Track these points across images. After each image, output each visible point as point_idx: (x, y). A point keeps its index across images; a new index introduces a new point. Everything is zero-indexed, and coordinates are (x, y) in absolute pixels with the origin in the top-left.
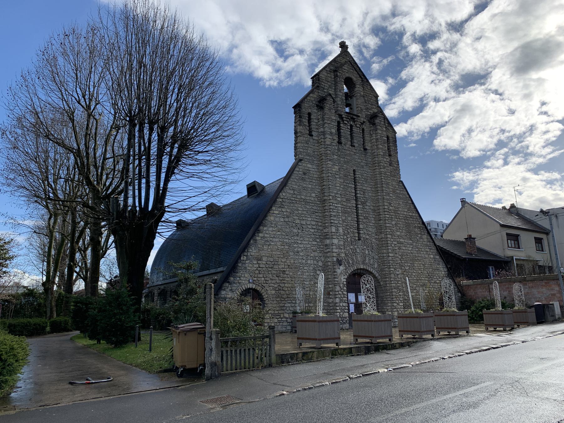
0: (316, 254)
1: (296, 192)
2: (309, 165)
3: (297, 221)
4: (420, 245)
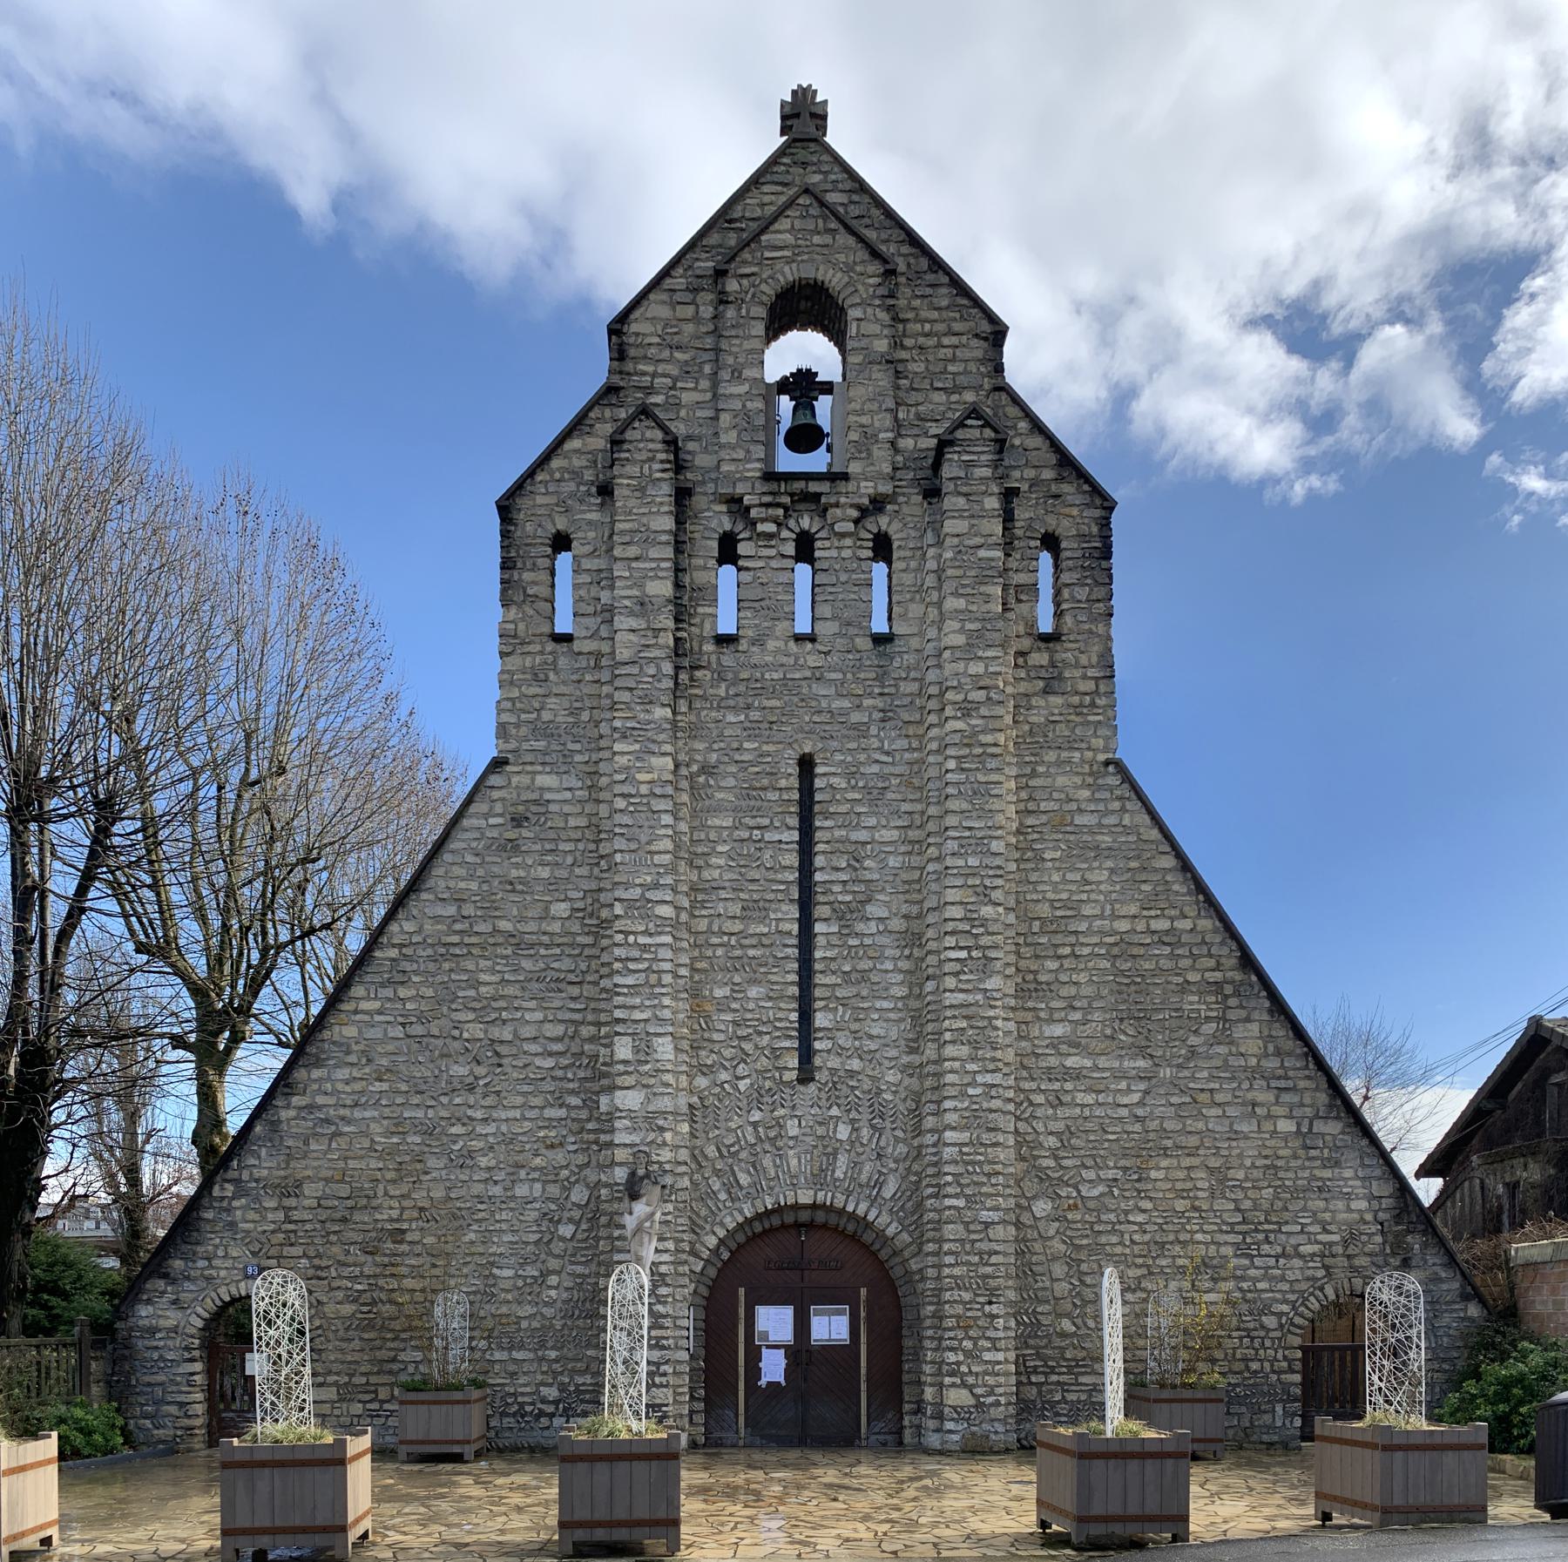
0: (559, 1157)
1: (468, 910)
2: (542, 780)
3: (476, 1031)
4: (1205, 1074)
